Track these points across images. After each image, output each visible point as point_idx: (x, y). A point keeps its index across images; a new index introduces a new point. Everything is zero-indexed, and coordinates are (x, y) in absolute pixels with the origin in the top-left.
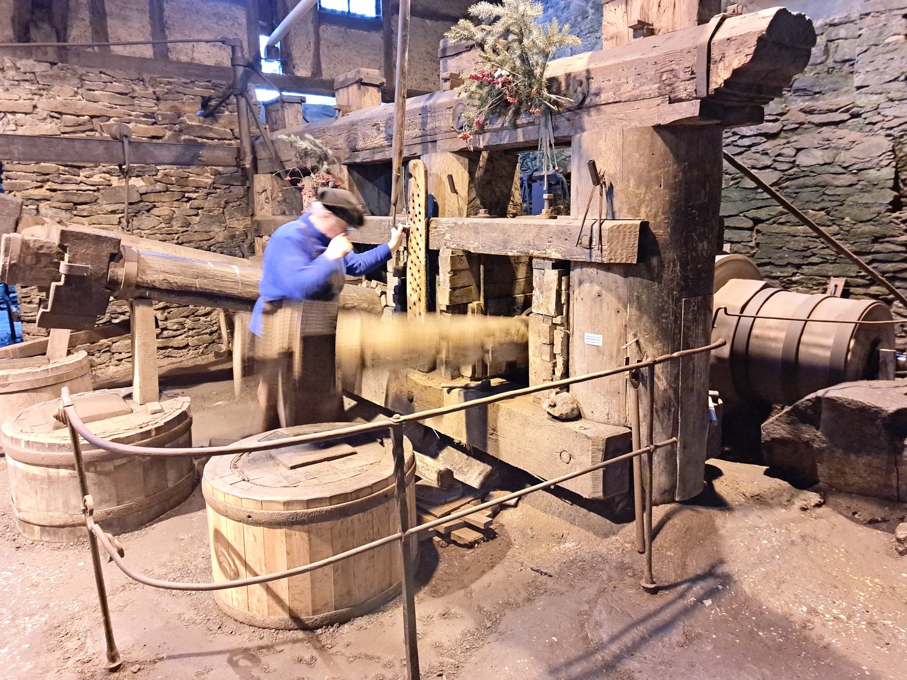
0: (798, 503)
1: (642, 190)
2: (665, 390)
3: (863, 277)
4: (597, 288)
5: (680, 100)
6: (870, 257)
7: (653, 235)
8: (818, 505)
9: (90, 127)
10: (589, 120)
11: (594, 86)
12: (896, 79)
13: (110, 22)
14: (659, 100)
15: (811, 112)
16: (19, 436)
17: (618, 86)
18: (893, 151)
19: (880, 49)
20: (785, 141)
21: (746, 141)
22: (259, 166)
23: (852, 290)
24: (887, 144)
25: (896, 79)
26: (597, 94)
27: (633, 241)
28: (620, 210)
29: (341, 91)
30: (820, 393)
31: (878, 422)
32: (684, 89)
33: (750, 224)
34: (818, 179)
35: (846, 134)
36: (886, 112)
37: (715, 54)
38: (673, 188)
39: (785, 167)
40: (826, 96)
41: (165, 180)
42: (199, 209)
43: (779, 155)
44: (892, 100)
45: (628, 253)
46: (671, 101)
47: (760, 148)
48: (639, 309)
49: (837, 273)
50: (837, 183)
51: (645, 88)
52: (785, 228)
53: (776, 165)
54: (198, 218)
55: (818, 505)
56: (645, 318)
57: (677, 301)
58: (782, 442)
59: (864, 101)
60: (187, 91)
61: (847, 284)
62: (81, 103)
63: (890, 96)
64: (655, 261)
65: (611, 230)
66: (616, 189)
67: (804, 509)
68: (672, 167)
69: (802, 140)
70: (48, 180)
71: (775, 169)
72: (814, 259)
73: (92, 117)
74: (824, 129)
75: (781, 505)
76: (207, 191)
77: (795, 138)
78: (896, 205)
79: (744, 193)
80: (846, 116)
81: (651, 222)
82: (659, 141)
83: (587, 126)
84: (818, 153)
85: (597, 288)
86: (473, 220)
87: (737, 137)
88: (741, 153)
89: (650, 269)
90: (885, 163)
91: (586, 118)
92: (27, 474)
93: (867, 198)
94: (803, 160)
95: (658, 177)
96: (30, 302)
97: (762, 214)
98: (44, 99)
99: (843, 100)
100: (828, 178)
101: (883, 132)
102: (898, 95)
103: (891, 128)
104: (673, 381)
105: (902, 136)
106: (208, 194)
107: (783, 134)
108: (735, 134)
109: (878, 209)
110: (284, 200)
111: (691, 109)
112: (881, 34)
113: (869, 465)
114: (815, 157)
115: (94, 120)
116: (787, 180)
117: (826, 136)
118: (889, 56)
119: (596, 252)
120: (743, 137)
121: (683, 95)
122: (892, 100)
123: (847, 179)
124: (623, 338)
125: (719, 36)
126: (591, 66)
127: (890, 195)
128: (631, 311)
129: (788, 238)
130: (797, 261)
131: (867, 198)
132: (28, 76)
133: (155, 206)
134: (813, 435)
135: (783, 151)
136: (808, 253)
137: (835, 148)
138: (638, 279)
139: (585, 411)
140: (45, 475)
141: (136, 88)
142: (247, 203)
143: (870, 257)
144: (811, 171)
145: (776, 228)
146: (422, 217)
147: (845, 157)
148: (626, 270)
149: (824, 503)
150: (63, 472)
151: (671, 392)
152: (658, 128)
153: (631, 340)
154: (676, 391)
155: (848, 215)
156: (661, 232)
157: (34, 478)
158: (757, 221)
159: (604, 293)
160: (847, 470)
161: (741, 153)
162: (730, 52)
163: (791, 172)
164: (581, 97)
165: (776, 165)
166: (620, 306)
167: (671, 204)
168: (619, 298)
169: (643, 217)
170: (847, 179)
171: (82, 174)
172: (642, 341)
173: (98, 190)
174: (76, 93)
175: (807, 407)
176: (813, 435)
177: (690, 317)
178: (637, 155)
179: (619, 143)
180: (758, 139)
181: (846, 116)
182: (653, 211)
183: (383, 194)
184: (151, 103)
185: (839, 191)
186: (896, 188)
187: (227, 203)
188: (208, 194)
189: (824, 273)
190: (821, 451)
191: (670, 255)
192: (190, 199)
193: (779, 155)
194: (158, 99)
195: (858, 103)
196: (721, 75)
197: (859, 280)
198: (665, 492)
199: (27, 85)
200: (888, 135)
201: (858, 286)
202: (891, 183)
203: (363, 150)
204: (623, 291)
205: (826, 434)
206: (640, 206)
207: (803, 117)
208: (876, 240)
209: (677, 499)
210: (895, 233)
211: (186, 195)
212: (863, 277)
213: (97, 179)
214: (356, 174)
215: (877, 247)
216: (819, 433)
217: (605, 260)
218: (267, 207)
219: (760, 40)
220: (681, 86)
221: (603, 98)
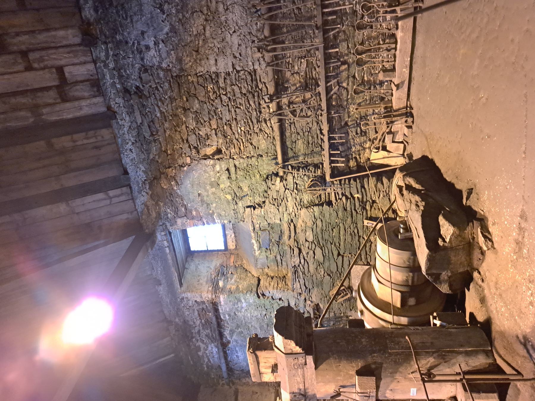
0: (480, 282)
1: (342, 373)
2: (434, 358)
3: (363, 213)
4: (388, 391)
5: (306, 361)
6: (353, 211)
7: (362, 367)
8: (479, 273)
10: (310, 392)
11: (296, 391)
12: (278, 210)
14: (305, 369)
15: (290, 237)
17: (298, 383)
18: (307, 208)
19: (266, 216)
20: (302, 246)
21: (302, 261)
23: (369, 216)
24: (304, 210)
25: (278, 210)
26: (300, 390)
27: (365, 379)
28: (351, 382)
30: (424, 273)
31: (434, 255)
33: (340, 257)
34: (319, 233)
35: (300, 224)
36: (291, 211)
37: (290, 352)
38: (340, 359)
39: (314, 245)
40: (283, 228)
43: (308, 248)
44: (286, 210)
45: (372, 381)
46: (306, 364)
47: (305, 256)
48: (396, 373)
49: (362, 222)
50: (321, 226)
51: (299, 373)
52: (342, 243)
53: (313, 249)
55: (479, 273)
56: (400, 370)
57: (390, 354)
58: (450, 286)
59: (286, 218)
61: (367, 219)
63: (284, 210)
64: (373, 366)
65: (361, 389)
66: (342, 384)
67: (483, 281)
68: (331, 361)
69: (302, 239)
71: (315, 249)
72: (356, 231)
74: (297, 231)
75: (483, 290)
77: (301, 242)
78: (330, 203)
79: (326, 261)
80: (292, 224)
81: (356, 369)
82: (321, 367)
83: (313, 393)
84: (308, 233)
87: (301, 265)
88: (308, 263)
89: (377, 368)
90: (312, 210)
91: (310, 393)
93: (327, 215)
94: (311, 239)
95: (336, 367)
97: (336, 253)
99: (285, 226)
100: (318, 230)
101: (299, 211)
102: (284, 209)
103: (298, 209)
104: (429, 354)
105: (301, 205)
107: (299, 246)
108: (299, 266)
109: (332, 211)
111: (310, 359)
112: (260, 216)
113: (455, 256)
114: (309, 235)
116: (319, 244)
117: (300, 231)
118: (269, 213)
119: (371, 394)
120: (300, 262)
121: (304, 361)
122: (286, 210)
123: (319, 222)
124: (410, 380)
125: (283, 350)
126: (288, 391)
127: (325, 207)
128: (398, 376)
129: (346, 242)
130: (357, 238)
131: (327, 215)
134: (445, 275)
135: (307, 246)
136: (353, 234)
137: (306, 227)
138: (382, 374)
139: (452, 395)
143: (353, 211)
144: (316, 236)
145: (342, 246)
147: (310, 224)
149: (478, 270)
151: (434, 355)
152: (316, 368)
153: (411, 376)
154: (434, 353)
155: (334, 221)
156: (360, 364)
158: (339, 254)
159: (390, 388)
160: (459, 263)
161: (308, 263)
162: (289, 347)
163: (316, 243)
164: (301, 396)
165: (313, 249)
166: (396, 381)
167: (347, 360)
168: (392, 381)
169: (354, 373)
170: (319, 222)
172: (411, 371)
175: (431, 277)
176: (445, 275)
177: (397, 347)
178: (327, 376)
179: (322, 384)
180: (301, 257)
181: (292, 224)
182: (351, 368)
185: (324, 225)
186: (322, 205)
189: (362, 227)
190: (452, 272)
191: (370, 359)
193: (308, 248)
195: (287, 220)
196: (298, 349)
197: (364, 214)
198: (487, 355)
200: (300, 209)
201: (367, 214)
202: (320, 207)
204: (388, 380)
205: (444, 271)
206: (349, 374)
207: (292, 239)
208: (345, 210)
210: (342, 204)
212: (363, 213)
215: (348, 209)
216: (444, 273)
217: (375, 391)
219: (286, 338)
220: (300, 361)
221: (302, 387)
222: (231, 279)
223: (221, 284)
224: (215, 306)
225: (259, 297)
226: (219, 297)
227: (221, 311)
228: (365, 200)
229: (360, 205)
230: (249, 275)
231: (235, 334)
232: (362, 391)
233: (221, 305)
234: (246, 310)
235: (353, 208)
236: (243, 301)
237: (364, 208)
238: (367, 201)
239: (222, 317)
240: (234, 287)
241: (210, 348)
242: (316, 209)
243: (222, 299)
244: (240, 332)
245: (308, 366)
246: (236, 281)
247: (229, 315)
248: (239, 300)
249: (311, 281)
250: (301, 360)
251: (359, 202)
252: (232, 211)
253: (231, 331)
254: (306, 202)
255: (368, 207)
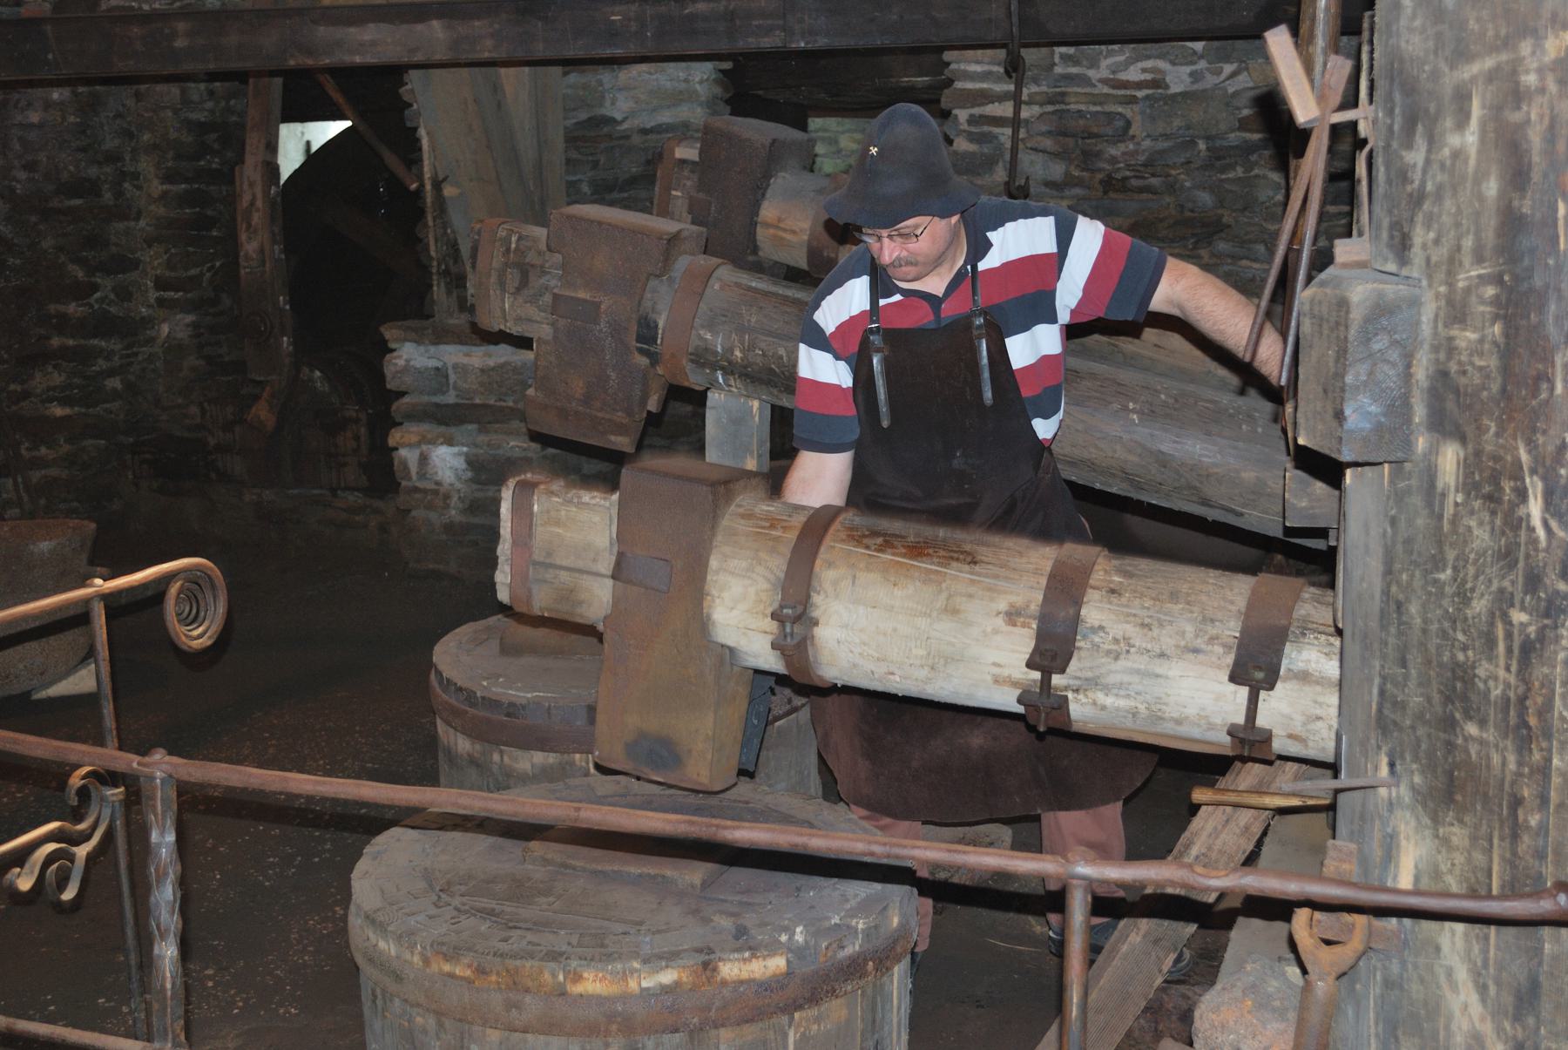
213: (1133, 74)
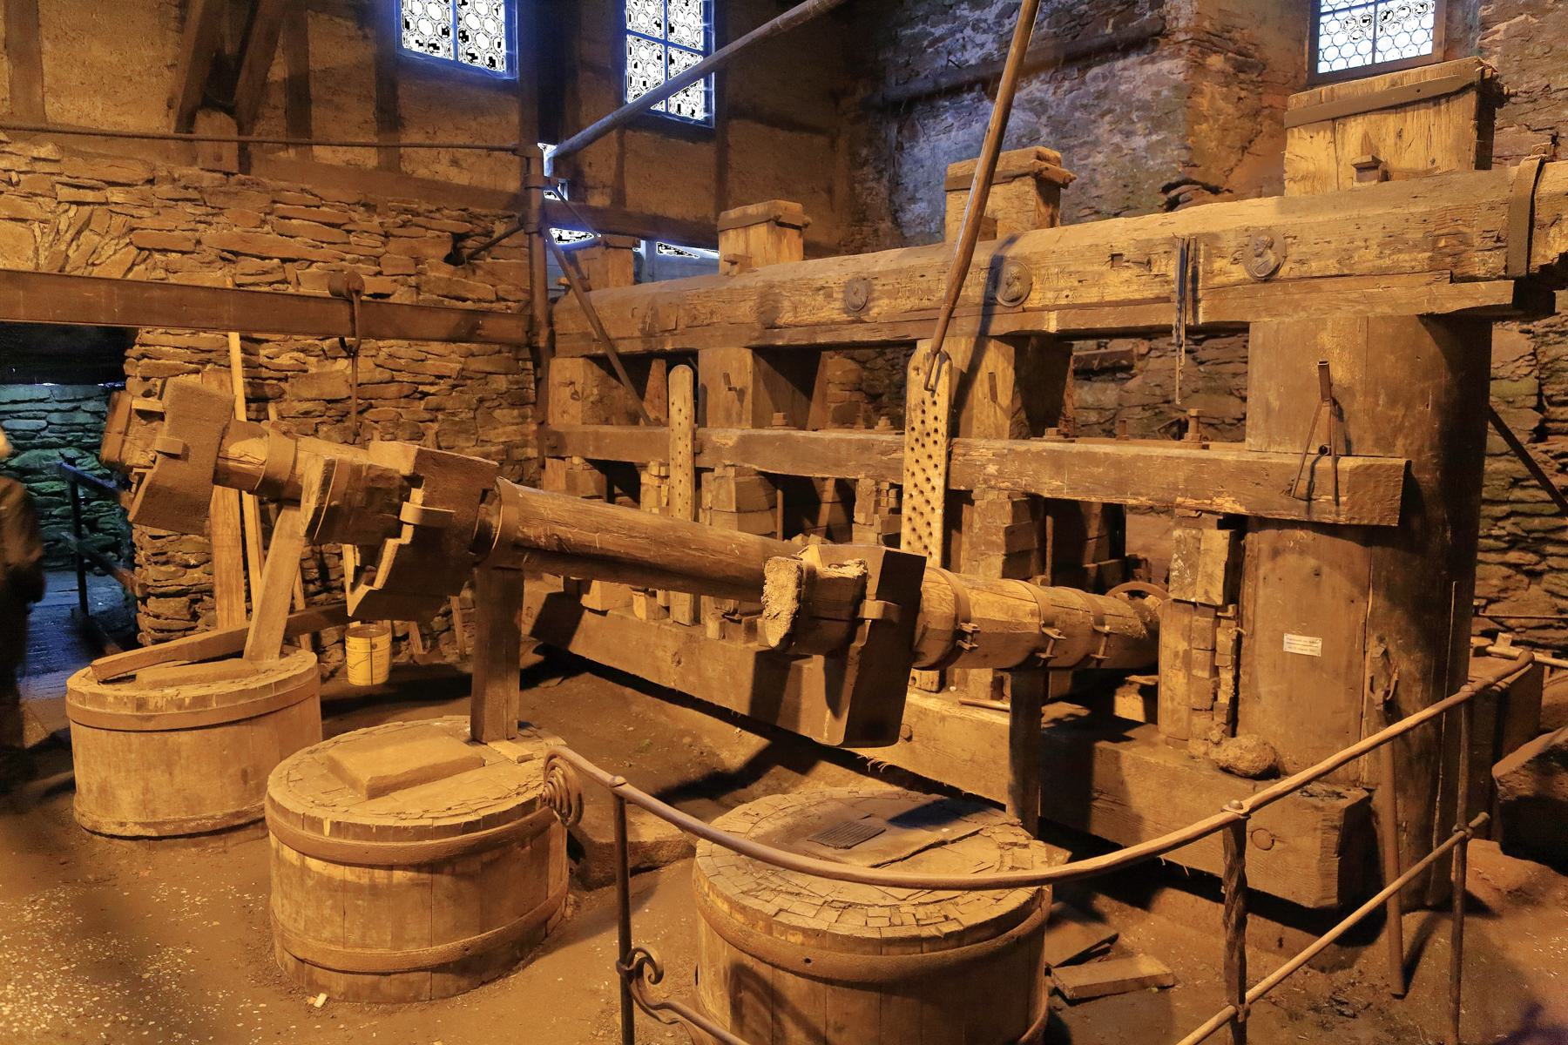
1: (1399, 412)
6: (1507, 508)
9: (279, 277)
13: (316, 112)
16: (317, 813)
18: (1534, 354)
22: (558, 346)
28: (1361, 440)
29: (731, 233)
32: (1483, 261)
37: (1543, 215)
41: (391, 363)
42: (438, 410)
46: (1453, 280)
51: (1402, 257)
54: (436, 426)
56: (1398, 613)
60: (434, 224)
62: (268, 238)
65: (1354, 472)
68: (1445, 378)
70: (209, 361)
73: (284, 260)
76: (451, 381)
85: (1312, 562)
86: (1035, 445)
90: (1526, 370)
92: (330, 879)
95: (1423, 393)
96: (166, 563)
98: (211, 231)
105: (1545, 334)
106: (454, 387)
110: (601, 400)
115: (288, 265)
132: (192, 194)
133: (371, 406)
138: (1389, 550)
140: (365, 881)
141: (356, 216)
142: (530, 399)
143: (1507, 508)
146: (941, 438)
148: (1367, 535)
150: (398, 875)
152: (1429, 320)
153: (1375, 650)
156: (1426, 478)
157: (344, 886)
159: (1326, 570)
166: (1356, 592)
168: (1354, 580)
171: (262, 352)
172: (1392, 649)
173: (286, 379)
174: (264, 222)
178: (1392, 358)
182: (1415, 447)
183: (798, 394)
184: (376, 241)
186: (1539, 408)
187: (481, 401)
188: (454, 387)
192: (426, 394)
194: (387, 235)
197: (1491, 542)
199: (189, 208)
202: (1533, 401)
203: (788, 326)
206: (1395, 437)
209: (1429, 903)
211: (421, 388)
212: (1497, 538)
214: (762, 362)
215: (1517, 494)
217: (1342, 520)
218: (576, 408)
222: (1226, 98)
223: (1215, 61)
224: (1144, 42)
225: (1166, 189)
226: (1174, 56)
227: (1120, 64)
228: (1550, 549)
229: (1529, 532)
230: (1233, 159)
231: (1030, 117)
232: (1343, 478)
233: (1142, 63)
234: (1118, 148)
235: (1519, 507)
236: (1154, 138)
237: (1514, 543)
238: (1544, 556)
239: (1096, 70)
240: (1204, 103)
241: (980, 38)
242: (1529, 384)
243: (1171, 67)
244: (1038, 131)
245: (1446, 288)
246: (1219, 112)
247: (1101, 95)
248: (1157, 125)
249: (1225, 357)
250: (1483, 261)
251: (1546, 531)
252: (1539, 82)
253: (1042, 103)
254: (1553, 352)
255: (1513, 557)
